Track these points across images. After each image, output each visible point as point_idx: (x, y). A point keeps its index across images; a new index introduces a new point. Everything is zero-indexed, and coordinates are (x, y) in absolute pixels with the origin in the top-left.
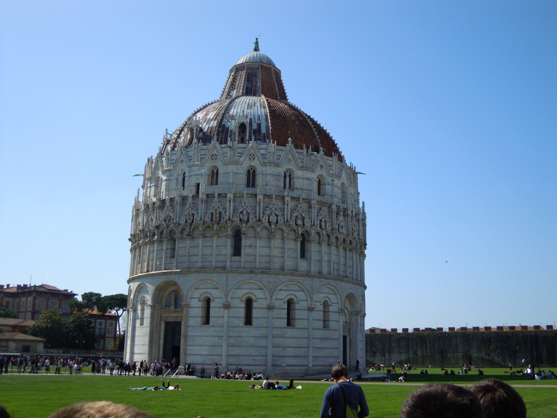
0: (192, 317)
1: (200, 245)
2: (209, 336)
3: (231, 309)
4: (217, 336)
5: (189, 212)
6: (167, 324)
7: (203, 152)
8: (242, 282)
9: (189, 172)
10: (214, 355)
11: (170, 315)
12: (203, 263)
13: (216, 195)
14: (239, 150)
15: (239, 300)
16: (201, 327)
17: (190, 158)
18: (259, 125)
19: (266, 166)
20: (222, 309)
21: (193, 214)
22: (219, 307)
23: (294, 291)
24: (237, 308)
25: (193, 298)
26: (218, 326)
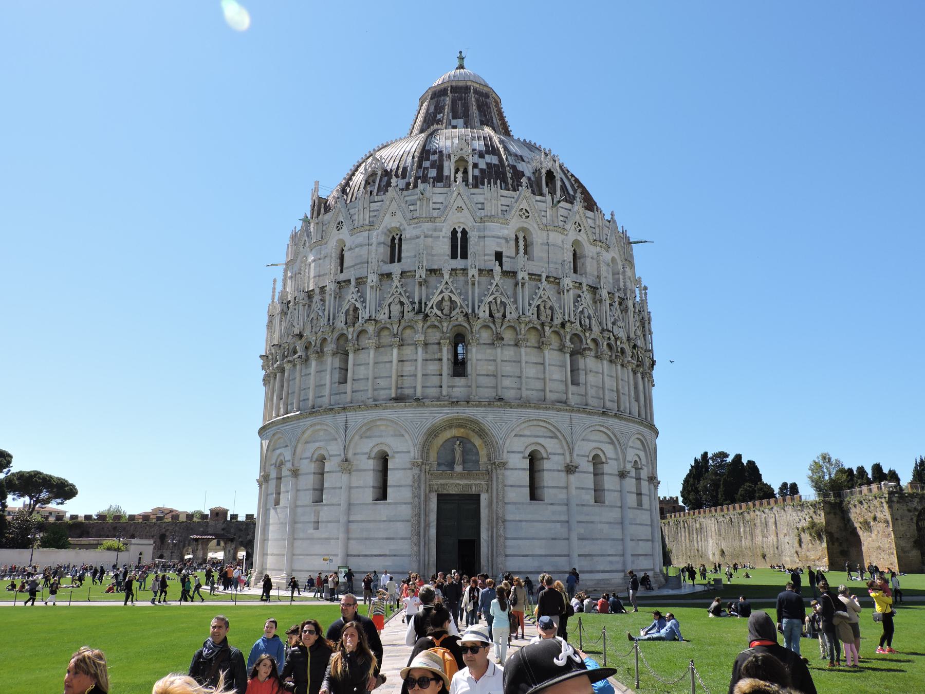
0: (511, 486)
1: (524, 358)
2: (545, 521)
3: (576, 474)
4: (558, 522)
5: (495, 299)
6: (442, 499)
7: (504, 201)
8: (591, 429)
10: (556, 556)
11: (451, 481)
12: (529, 392)
14: (562, 212)
15: (586, 459)
17: (480, 206)
20: (563, 474)
21: (504, 304)
22: (559, 471)
24: (585, 472)
25: (513, 452)
26: (559, 504)
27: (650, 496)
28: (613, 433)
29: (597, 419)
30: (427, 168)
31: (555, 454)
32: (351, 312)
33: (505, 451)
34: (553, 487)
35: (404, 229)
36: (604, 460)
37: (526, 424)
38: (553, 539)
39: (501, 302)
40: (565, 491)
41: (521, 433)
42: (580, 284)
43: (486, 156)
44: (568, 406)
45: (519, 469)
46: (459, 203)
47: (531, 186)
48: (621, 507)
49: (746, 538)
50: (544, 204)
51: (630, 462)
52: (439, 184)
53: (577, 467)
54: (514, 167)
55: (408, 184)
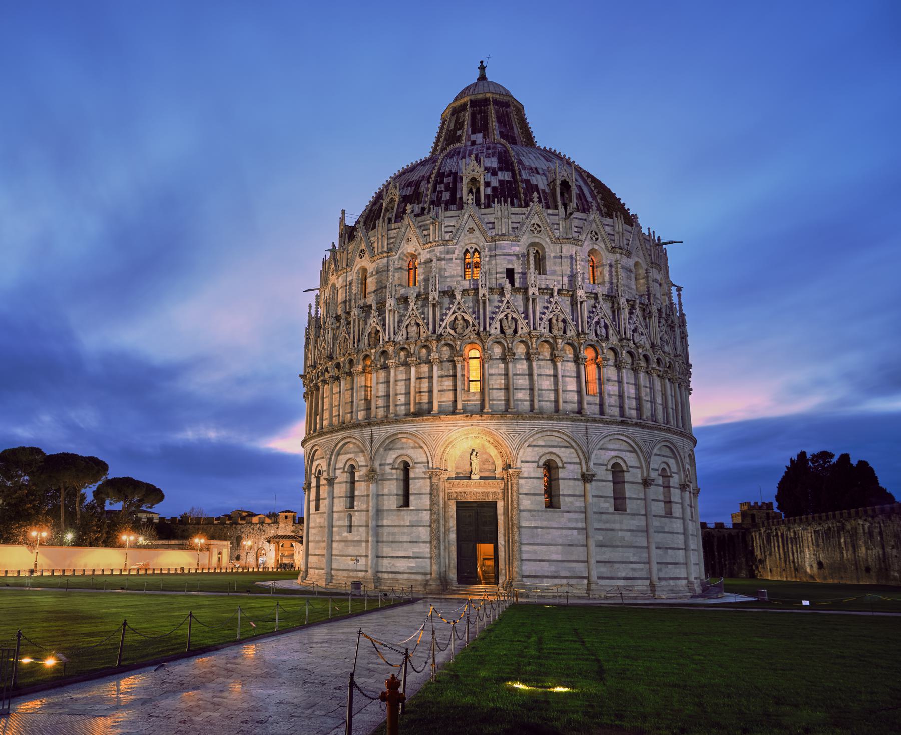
2: (562, 528)
3: (593, 483)
4: (575, 529)
5: (506, 316)
7: (514, 218)
8: (609, 438)
9: (490, 250)
13: (556, 289)
14: (576, 222)
16: (546, 512)
17: (490, 226)
18: (579, 187)
19: (614, 252)
20: (580, 483)
22: (575, 479)
23: (667, 457)
26: (575, 512)
27: (682, 504)
28: (633, 441)
29: (615, 428)
30: (441, 192)
31: (570, 463)
32: (373, 335)
33: (519, 461)
34: (569, 496)
35: (419, 254)
36: (625, 468)
37: (540, 435)
38: (570, 545)
39: (512, 318)
40: (583, 499)
41: (534, 443)
42: (596, 294)
43: (499, 173)
44: (583, 416)
45: (534, 478)
46: (471, 224)
47: (545, 199)
48: (646, 515)
49: (847, 551)
50: (557, 217)
51: (657, 470)
52: (452, 207)
53: (593, 476)
54: (527, 181)
55: (423, 209)
